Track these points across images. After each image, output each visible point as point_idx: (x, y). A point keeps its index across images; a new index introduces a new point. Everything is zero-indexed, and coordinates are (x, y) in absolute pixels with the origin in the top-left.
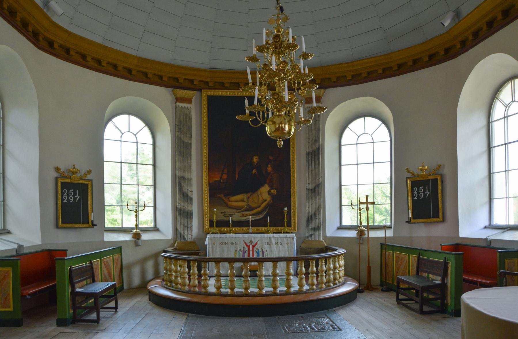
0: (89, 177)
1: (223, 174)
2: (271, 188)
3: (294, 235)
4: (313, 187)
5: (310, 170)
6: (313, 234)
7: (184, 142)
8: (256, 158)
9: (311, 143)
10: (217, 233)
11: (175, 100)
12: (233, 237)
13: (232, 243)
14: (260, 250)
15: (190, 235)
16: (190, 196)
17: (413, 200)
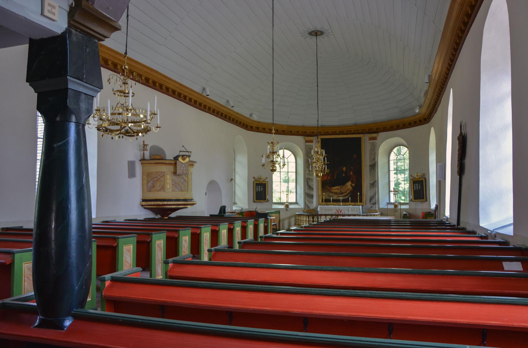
0: (267, 180)
5: (371, 174)
9: (371, 160)
10: (325, 205)
11: (305, 142)
17: (414, 190)
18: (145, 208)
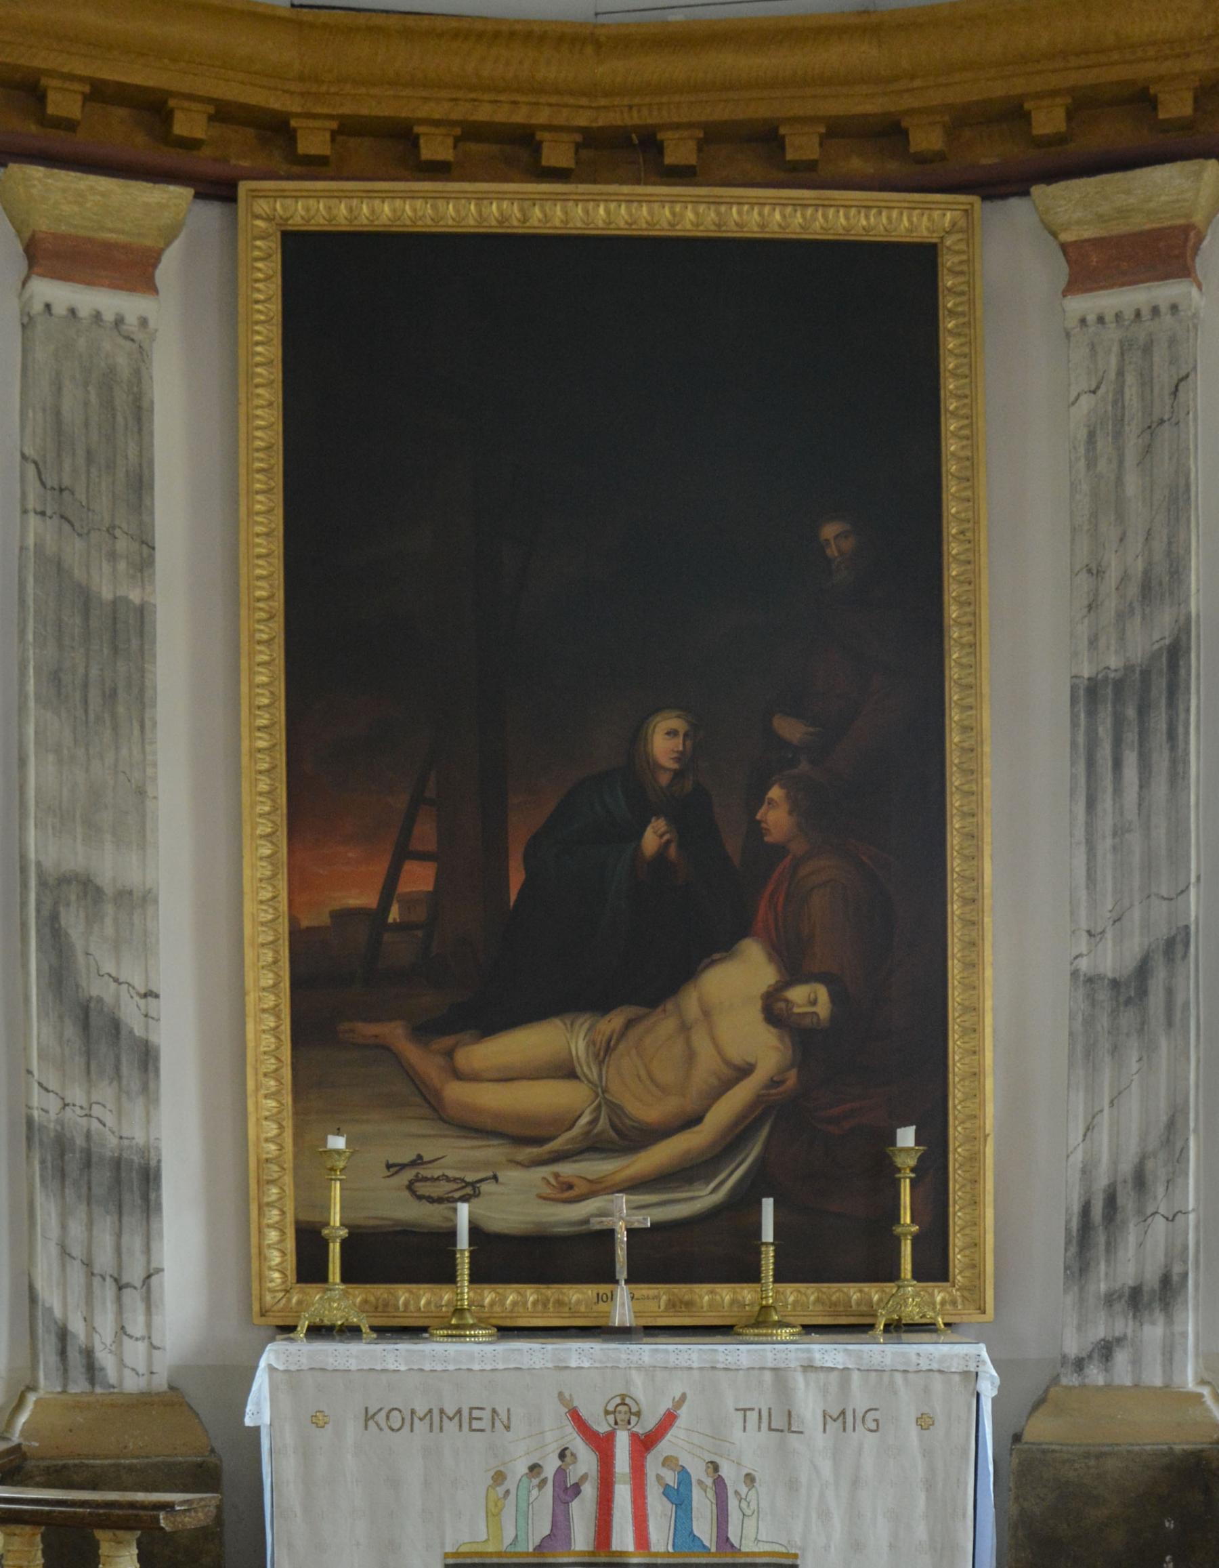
1: (402, 854)
3: (982, 1350)
4: (1130, 963)
5: (1106, 823)
6: (1120, 1341)
7: (86, 599)
8: (672, 733)
9: (1111, 605)
10: (351, 1332)
12: (476, 1367)
13: (466, 1418)
14: (698, 1471)
15: (142, 1346)
16: (138, 1032)
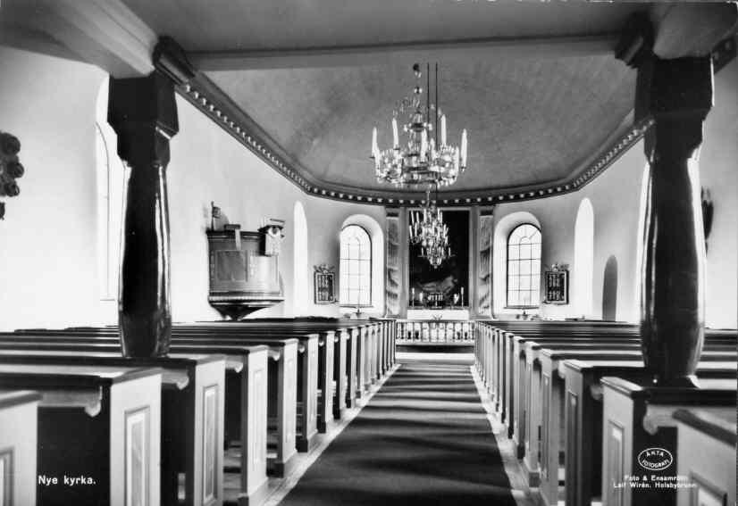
2: (455, 278)
18: (213, 306)
